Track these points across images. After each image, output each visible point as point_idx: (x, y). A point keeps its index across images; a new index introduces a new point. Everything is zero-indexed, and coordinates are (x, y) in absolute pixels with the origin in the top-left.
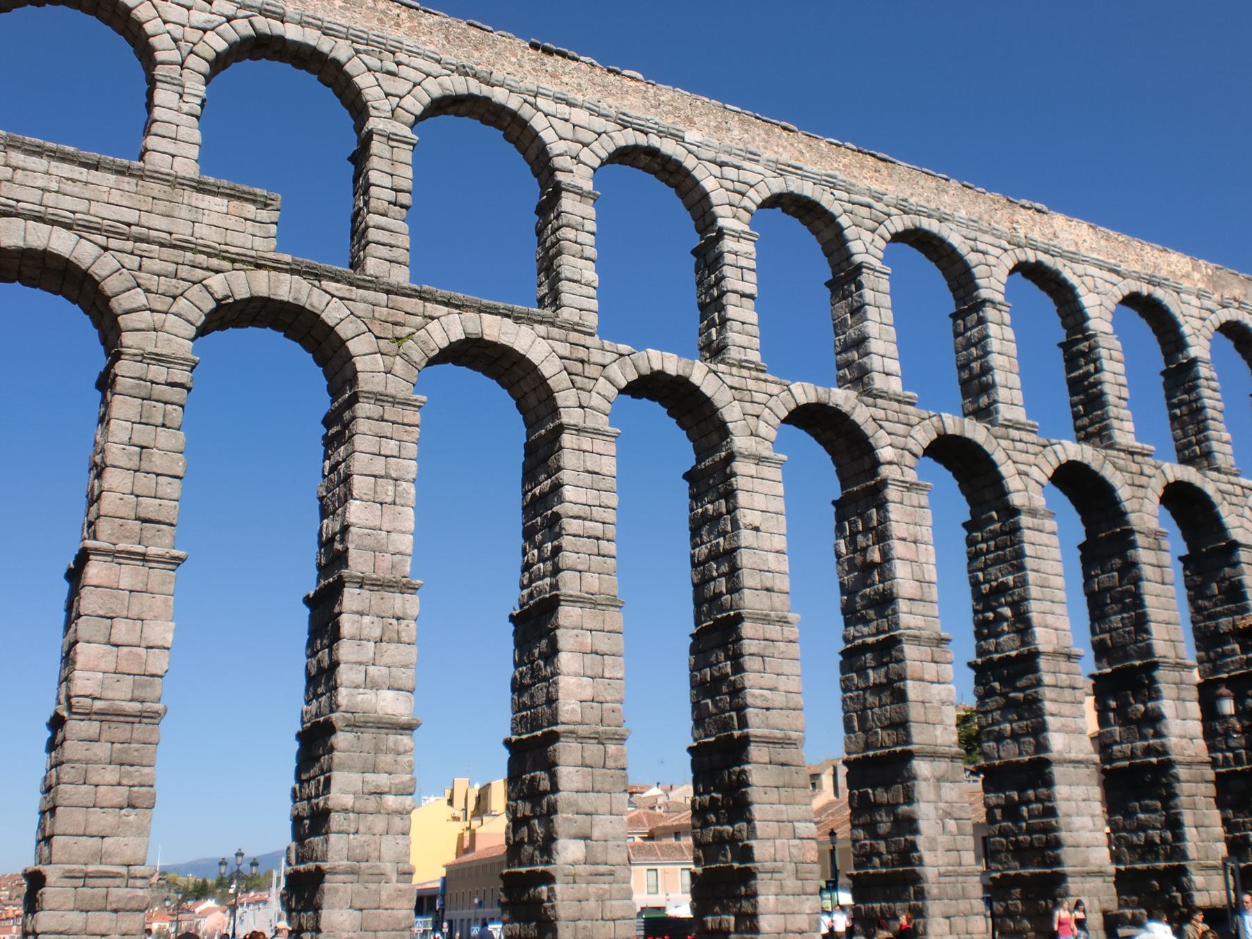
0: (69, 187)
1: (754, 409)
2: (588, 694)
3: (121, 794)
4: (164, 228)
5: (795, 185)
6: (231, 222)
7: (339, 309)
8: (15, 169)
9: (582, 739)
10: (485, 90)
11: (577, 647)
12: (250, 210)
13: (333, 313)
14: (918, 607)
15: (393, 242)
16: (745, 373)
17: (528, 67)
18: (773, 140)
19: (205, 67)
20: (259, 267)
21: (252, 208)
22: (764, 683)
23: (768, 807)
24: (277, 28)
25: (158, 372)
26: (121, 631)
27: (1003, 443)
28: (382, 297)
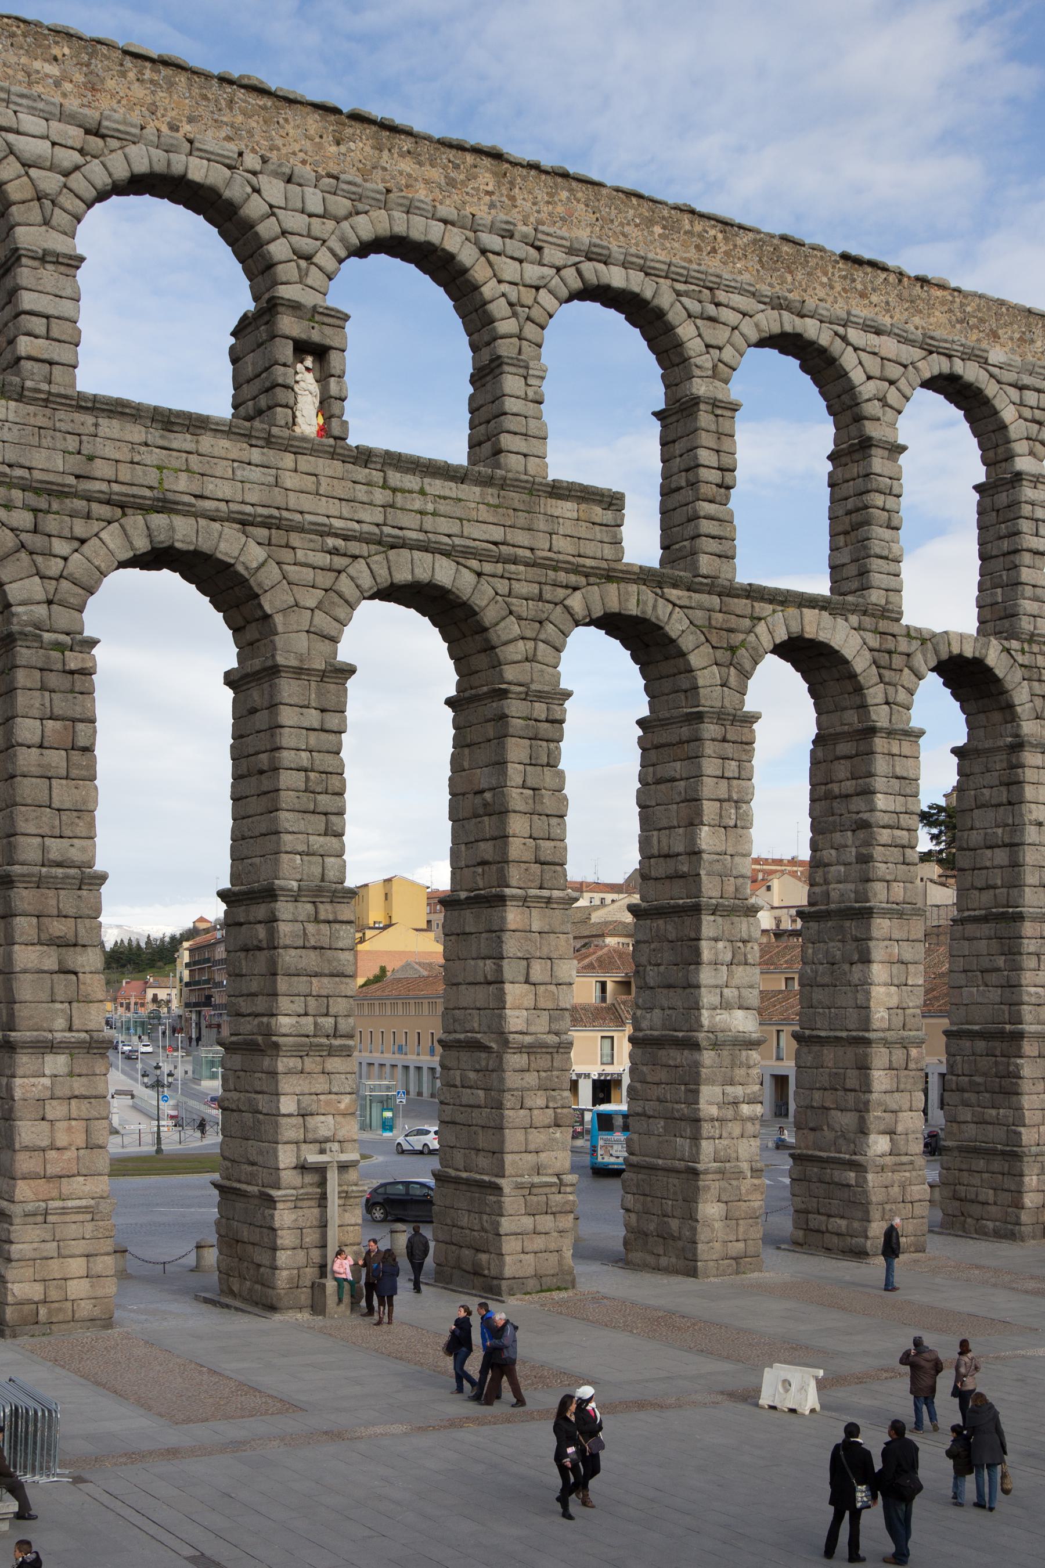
0: (443, 507)
2: (894, 1002)
4: (526, 544)
6: (583, 530)
7: (680, 621)
8: (394, 490)
9: (887, 1043)
11: (886, 958)
12: (598, 513)
13: (676, 625)
15: (722, 534)
20: (609, 579)
21: (598, 510)
23: (1035, 1097)
25: (540, 709)
28: (716, 600)
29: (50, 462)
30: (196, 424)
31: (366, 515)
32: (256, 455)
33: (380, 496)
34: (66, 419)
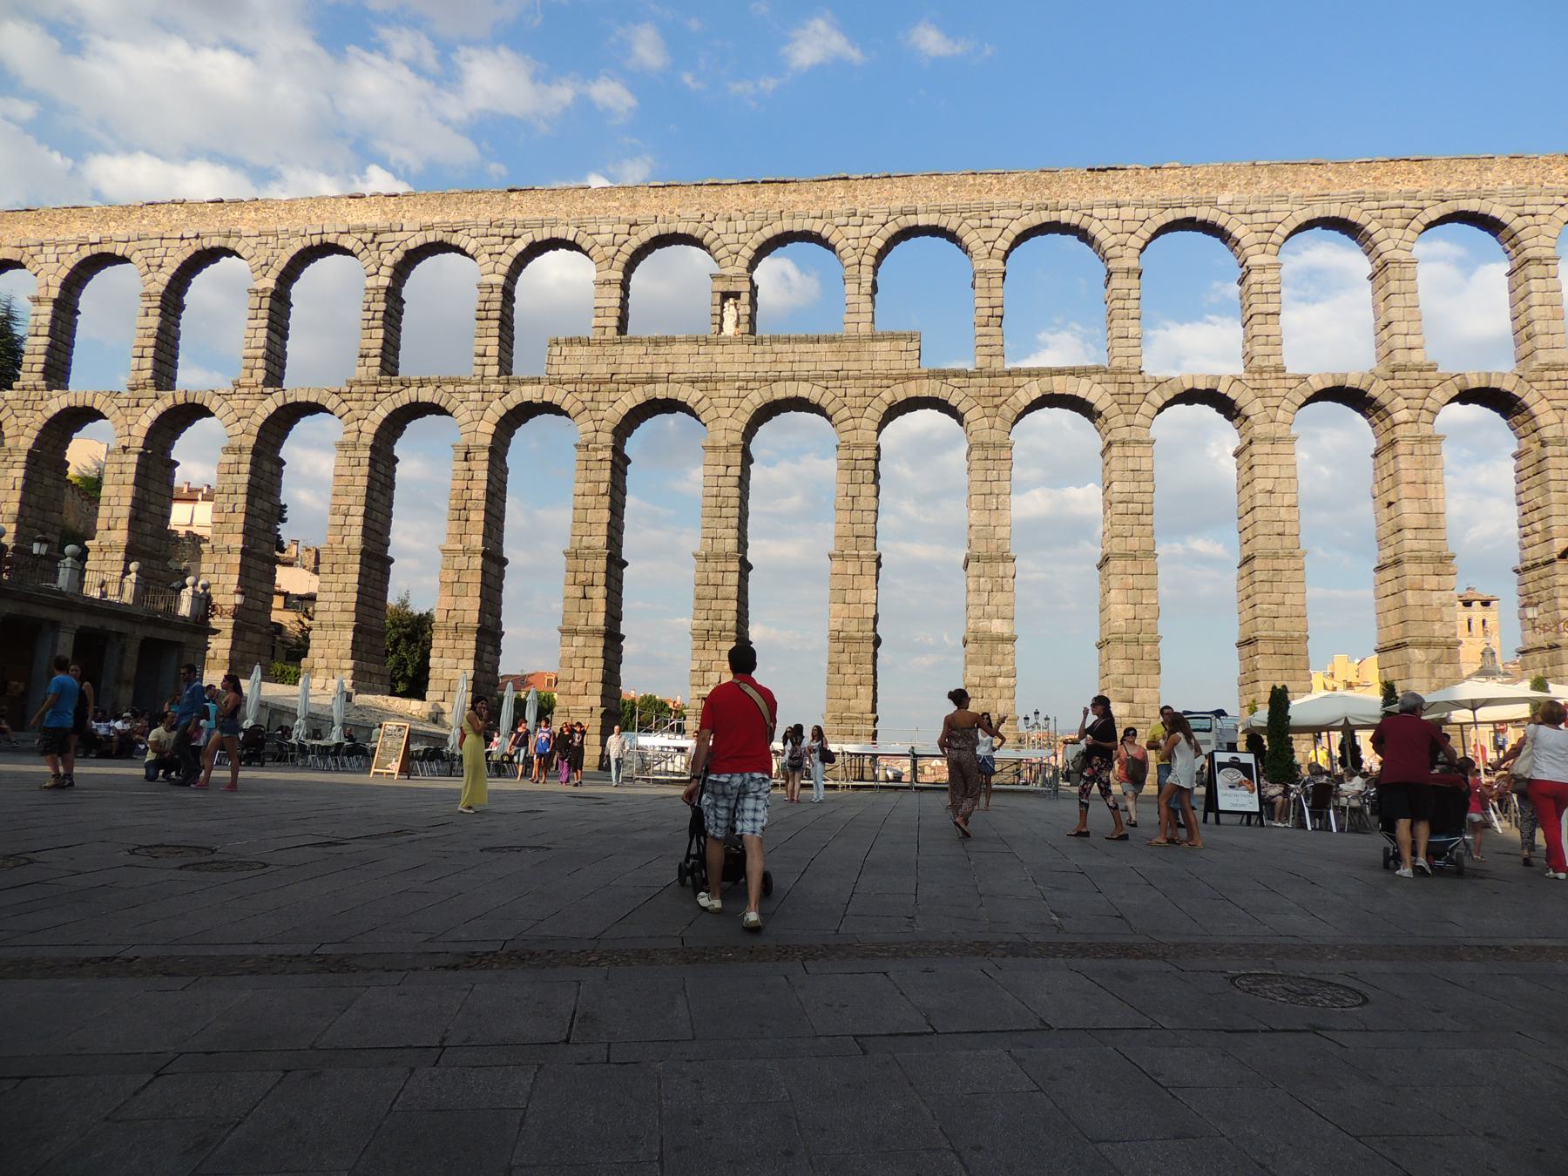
0: (805, 357)
1: (1275, 402)
2: (1131, 615)
3: (855, 679)
5: (1318, 212)
9: (1127, 643)
10: (1054, 217)
12: (903, 345)
14: (1426, 534)
16: (1265, 376)
17: (1086, 188)
18: (1301, 177)
19: (872, 261)
22: (1269, 600)
24: (912, 221)
25: (857, 454)
26: (850, 596)
27: (1537, 385)
29: (602, 370)
30: (670, 341)
31: (760, 368)
32: (702, 349)
33: (768, 358)
34: (609, 350)
